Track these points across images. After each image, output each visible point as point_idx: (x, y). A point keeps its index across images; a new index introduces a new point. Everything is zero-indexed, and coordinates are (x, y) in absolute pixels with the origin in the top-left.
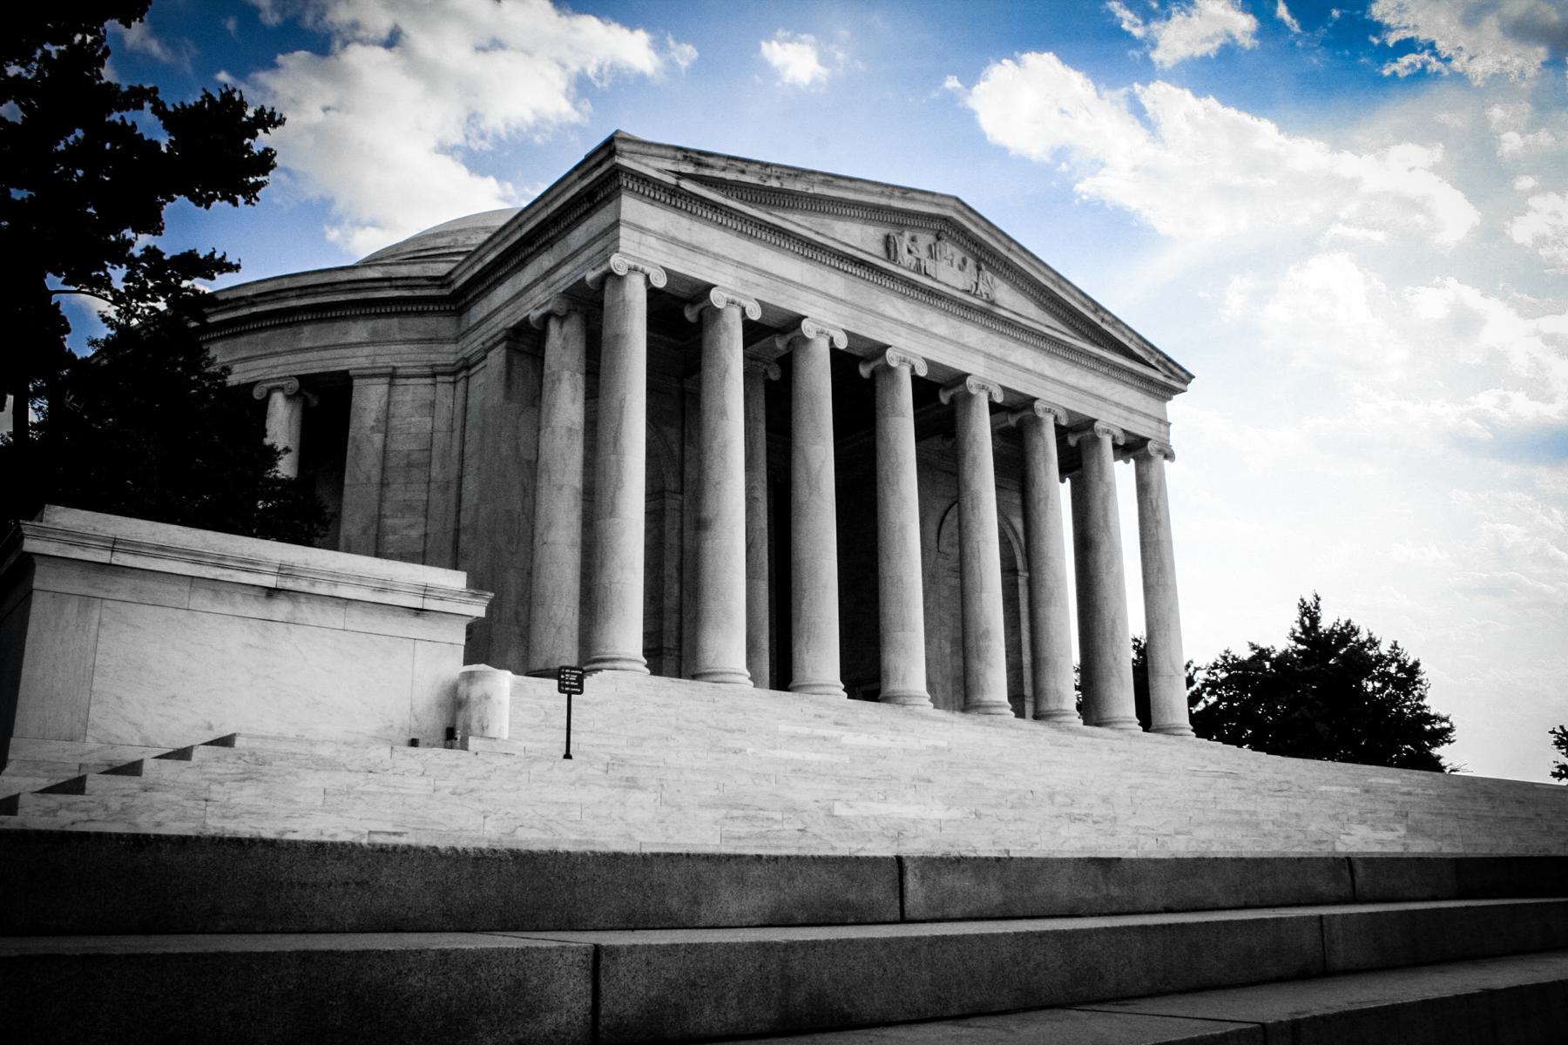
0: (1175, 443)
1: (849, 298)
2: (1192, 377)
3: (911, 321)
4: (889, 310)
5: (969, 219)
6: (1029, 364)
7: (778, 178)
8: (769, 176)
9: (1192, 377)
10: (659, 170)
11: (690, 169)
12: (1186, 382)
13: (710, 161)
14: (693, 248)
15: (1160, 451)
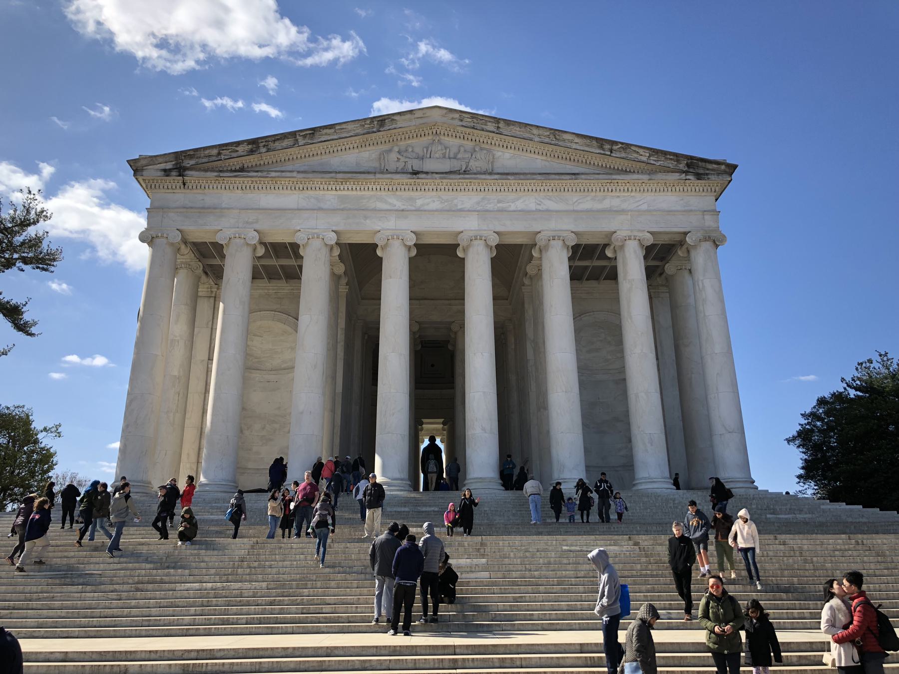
0: (723, 230)
1: (342, 207)
2: (735, 167)
3: (403, 207)
4: (380, 205)
5: (453, 119)
6: (533, 207)
7: (264, 146)
8: (258, 147)
9: (735, 167)
10: (165, 170)
11: (192, 162)
12: (731, 174)
13: (207, 152)
14: (205, 210)
15: (706, 239)
